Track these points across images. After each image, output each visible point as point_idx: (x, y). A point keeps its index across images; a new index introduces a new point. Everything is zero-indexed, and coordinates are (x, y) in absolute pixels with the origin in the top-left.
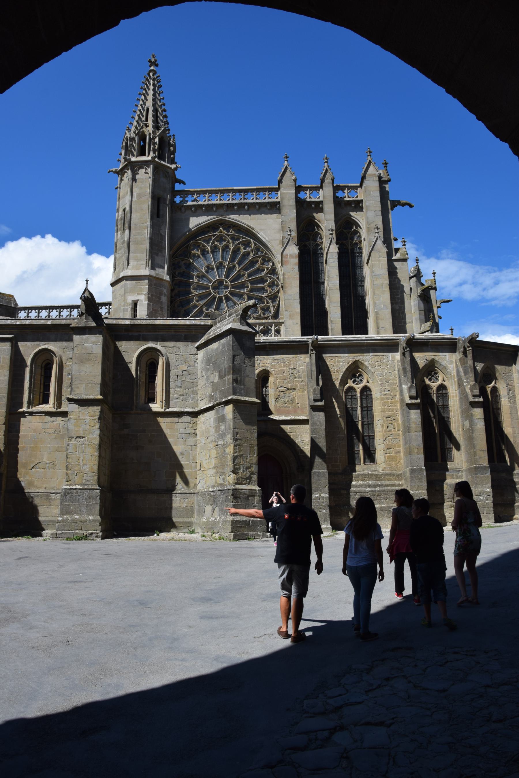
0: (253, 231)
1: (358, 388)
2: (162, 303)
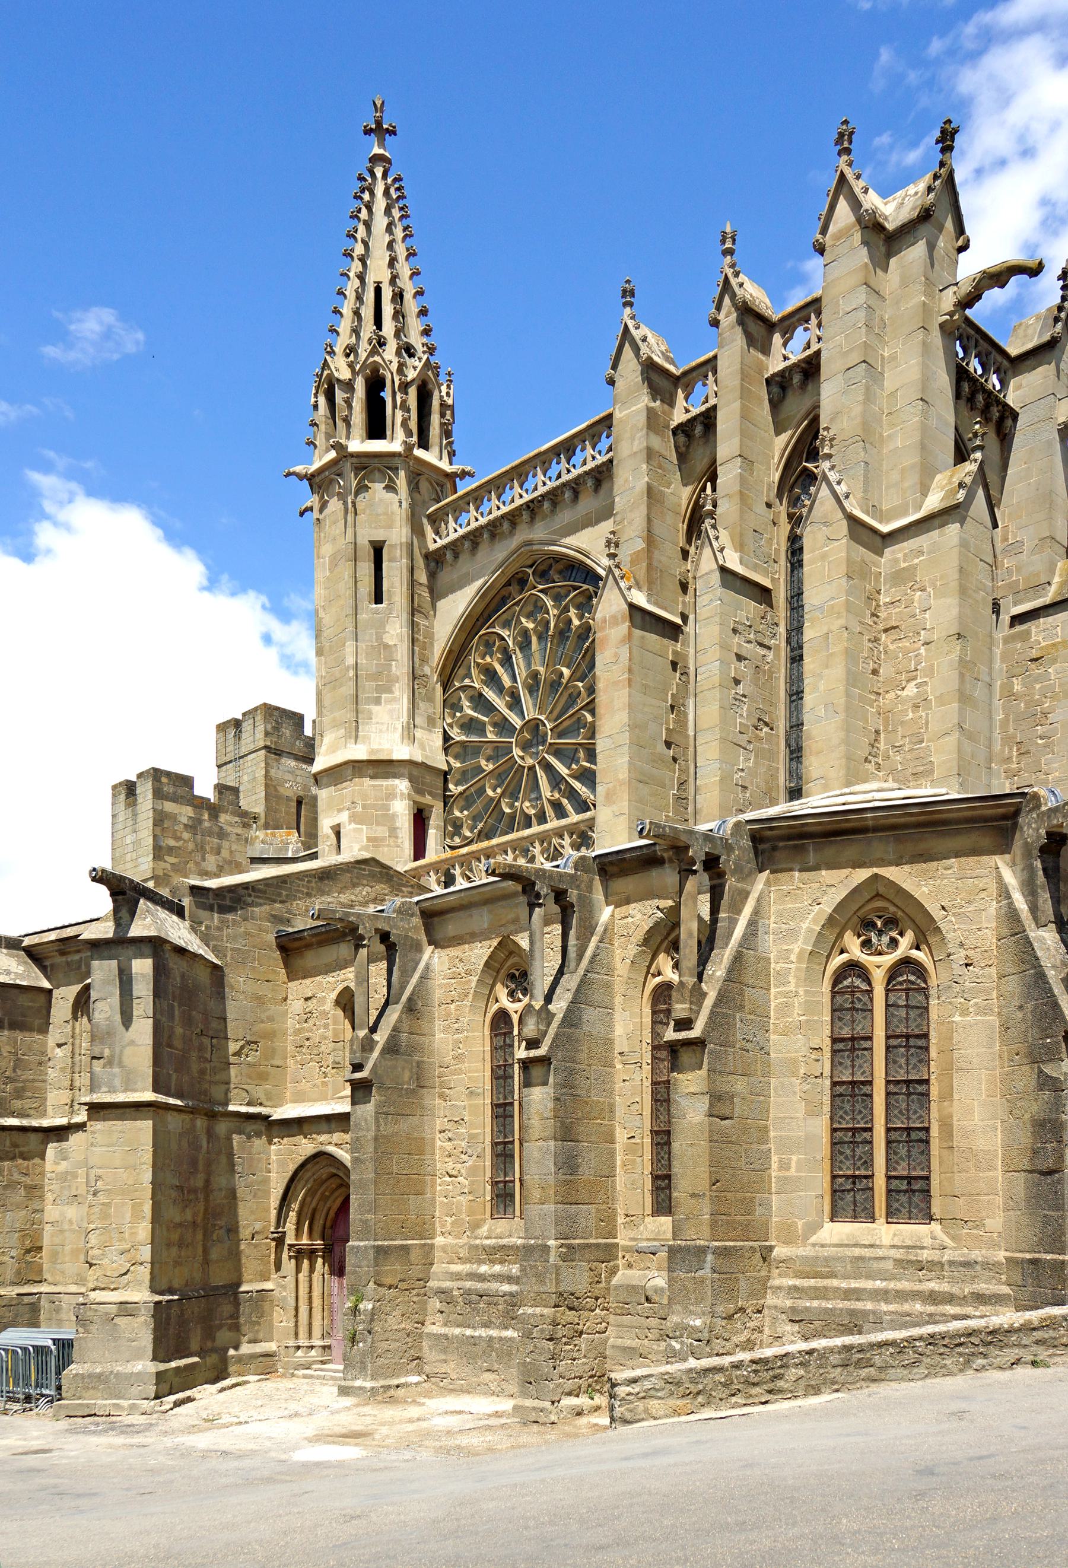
0: (588, 562)
1: (516, 1012)
2: (393, 817)
